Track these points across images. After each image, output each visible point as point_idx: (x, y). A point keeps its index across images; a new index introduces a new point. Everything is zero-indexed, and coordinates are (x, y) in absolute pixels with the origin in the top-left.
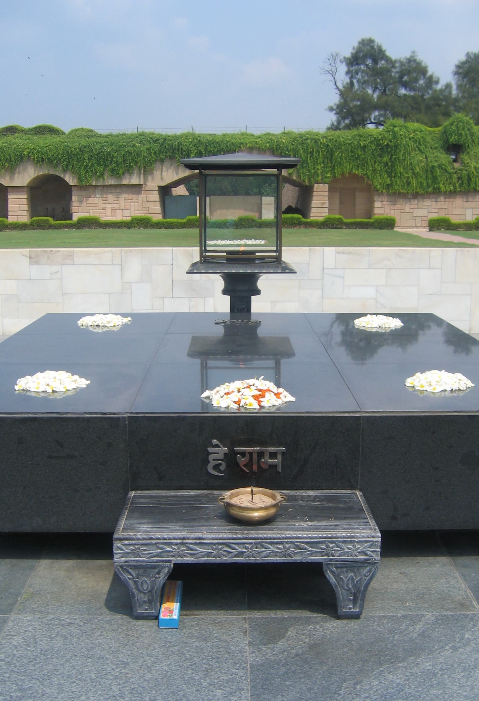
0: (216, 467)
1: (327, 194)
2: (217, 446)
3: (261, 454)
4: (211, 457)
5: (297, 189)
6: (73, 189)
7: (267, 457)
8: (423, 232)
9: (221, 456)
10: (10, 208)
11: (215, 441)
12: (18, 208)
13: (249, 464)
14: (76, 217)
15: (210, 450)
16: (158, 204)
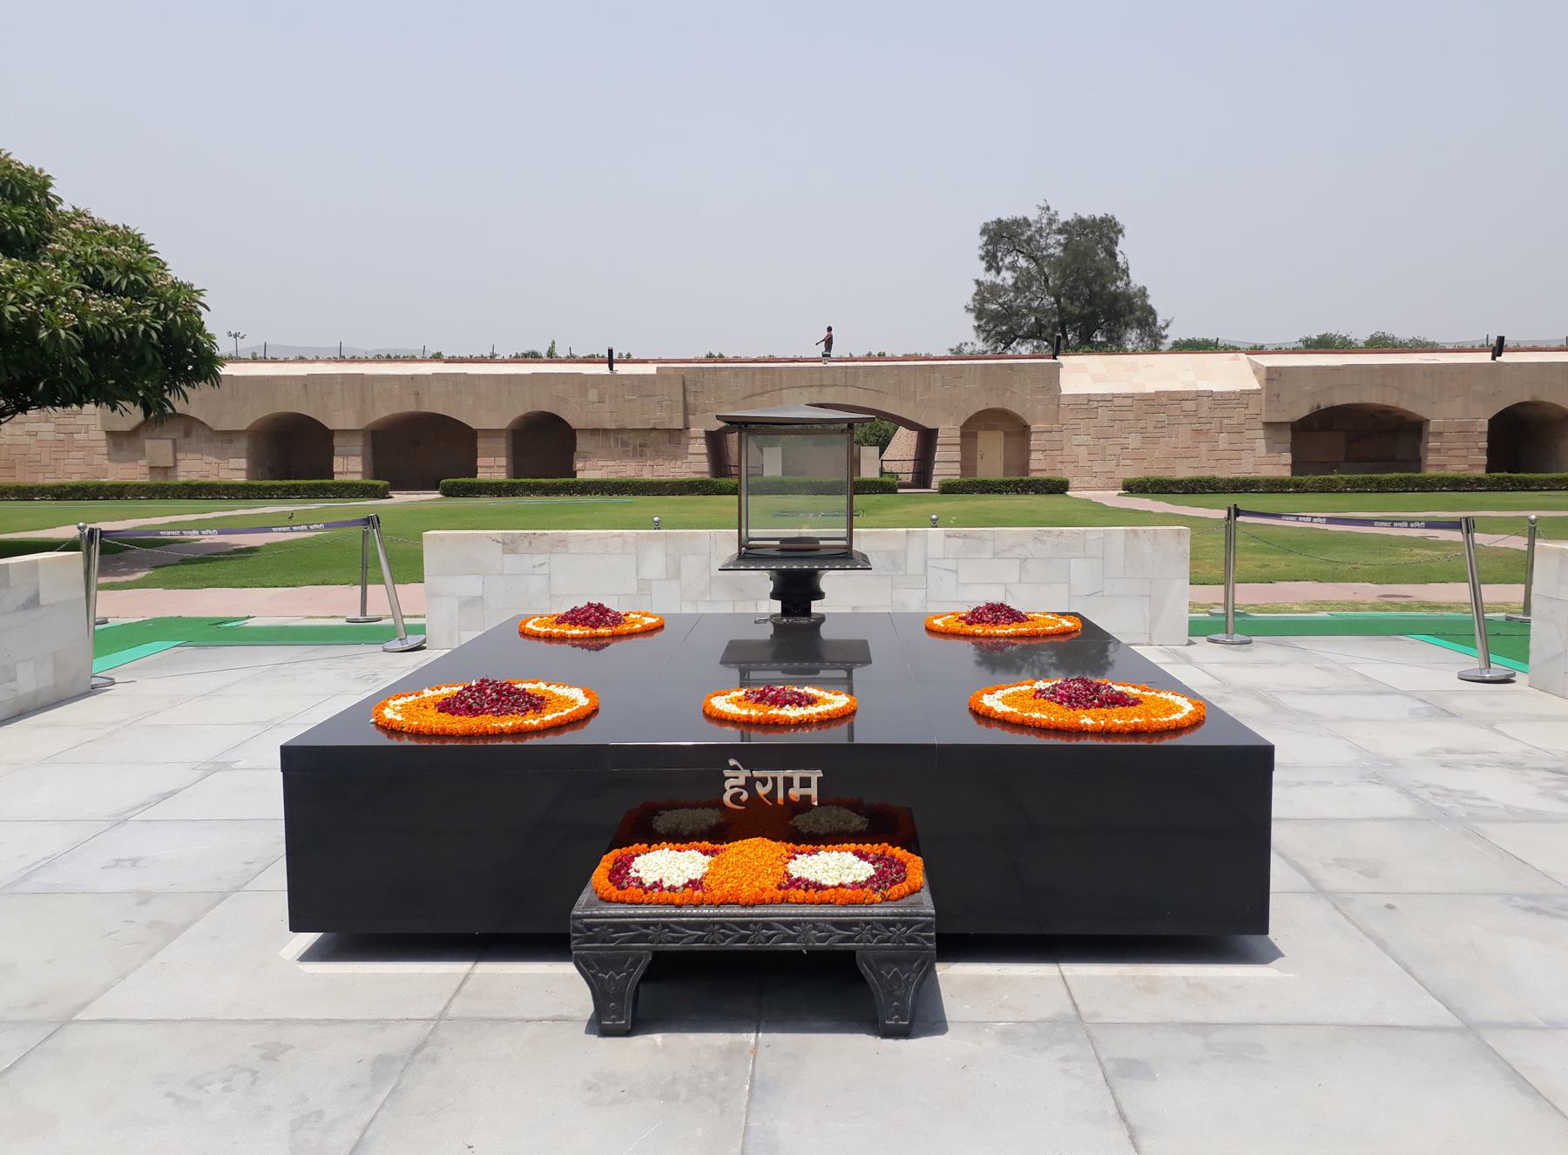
0: (735, 798)
1: (958, 441)
2: (735, 768)
3: (788, 783)
4: (728, 784)
5: (915, 433)
6: (578, 435)
7: (796, 782)
8: (1112, 498)
9: (742, 782)
10: (480, 461)
11: (732, 762)
12: (493, 466)
13: (772, 795)
14: (580, 476)
15: (727, 773)
16: (704, 458)
